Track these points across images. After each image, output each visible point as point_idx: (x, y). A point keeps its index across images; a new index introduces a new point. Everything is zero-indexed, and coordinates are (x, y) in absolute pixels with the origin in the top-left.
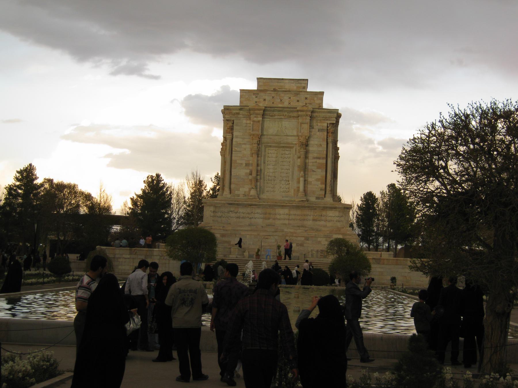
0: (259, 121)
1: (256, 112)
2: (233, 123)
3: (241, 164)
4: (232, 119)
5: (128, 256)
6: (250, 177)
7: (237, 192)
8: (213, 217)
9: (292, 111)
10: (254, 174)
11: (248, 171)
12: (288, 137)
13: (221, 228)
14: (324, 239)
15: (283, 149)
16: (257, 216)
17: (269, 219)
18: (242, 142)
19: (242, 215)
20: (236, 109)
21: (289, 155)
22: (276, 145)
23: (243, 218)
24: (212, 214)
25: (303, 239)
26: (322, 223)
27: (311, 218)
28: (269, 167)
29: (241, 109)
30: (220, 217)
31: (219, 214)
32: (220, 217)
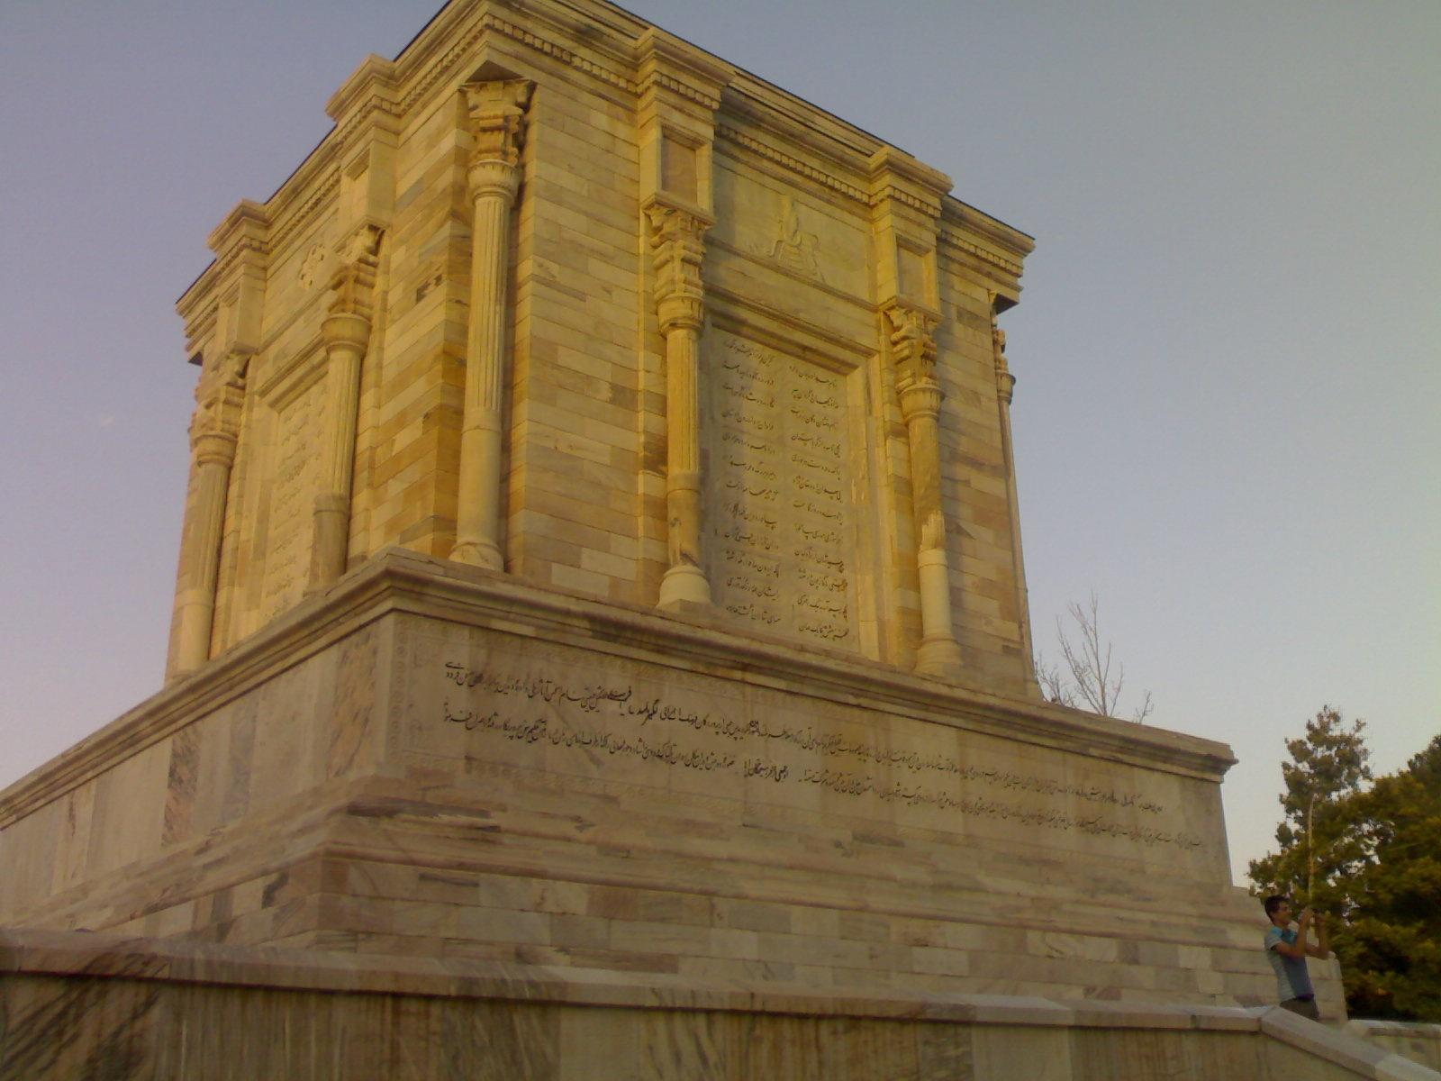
0: (694, 144)
1: (684, 78)
2: (526, 107)
3: (589, 379)
4: (529, 74)
6: (645, 483)
7: (560, 576)
8: (469, 723)
10: (682, 465)
12: (830, 301)
13: (569, 828)
15: (803, 366)
16: (782, 754)
17: (856, 790)
19: (687, 740)
20: (558, 24)
21: (829, 410)
22: (773, 326)
23: (693, 761)
24: (462, 701)
25: (1110, 950)
26: (1123, 847)
29: (585, 35)
30: (531, 734)
31: (516, 708)
32: (531, 734)
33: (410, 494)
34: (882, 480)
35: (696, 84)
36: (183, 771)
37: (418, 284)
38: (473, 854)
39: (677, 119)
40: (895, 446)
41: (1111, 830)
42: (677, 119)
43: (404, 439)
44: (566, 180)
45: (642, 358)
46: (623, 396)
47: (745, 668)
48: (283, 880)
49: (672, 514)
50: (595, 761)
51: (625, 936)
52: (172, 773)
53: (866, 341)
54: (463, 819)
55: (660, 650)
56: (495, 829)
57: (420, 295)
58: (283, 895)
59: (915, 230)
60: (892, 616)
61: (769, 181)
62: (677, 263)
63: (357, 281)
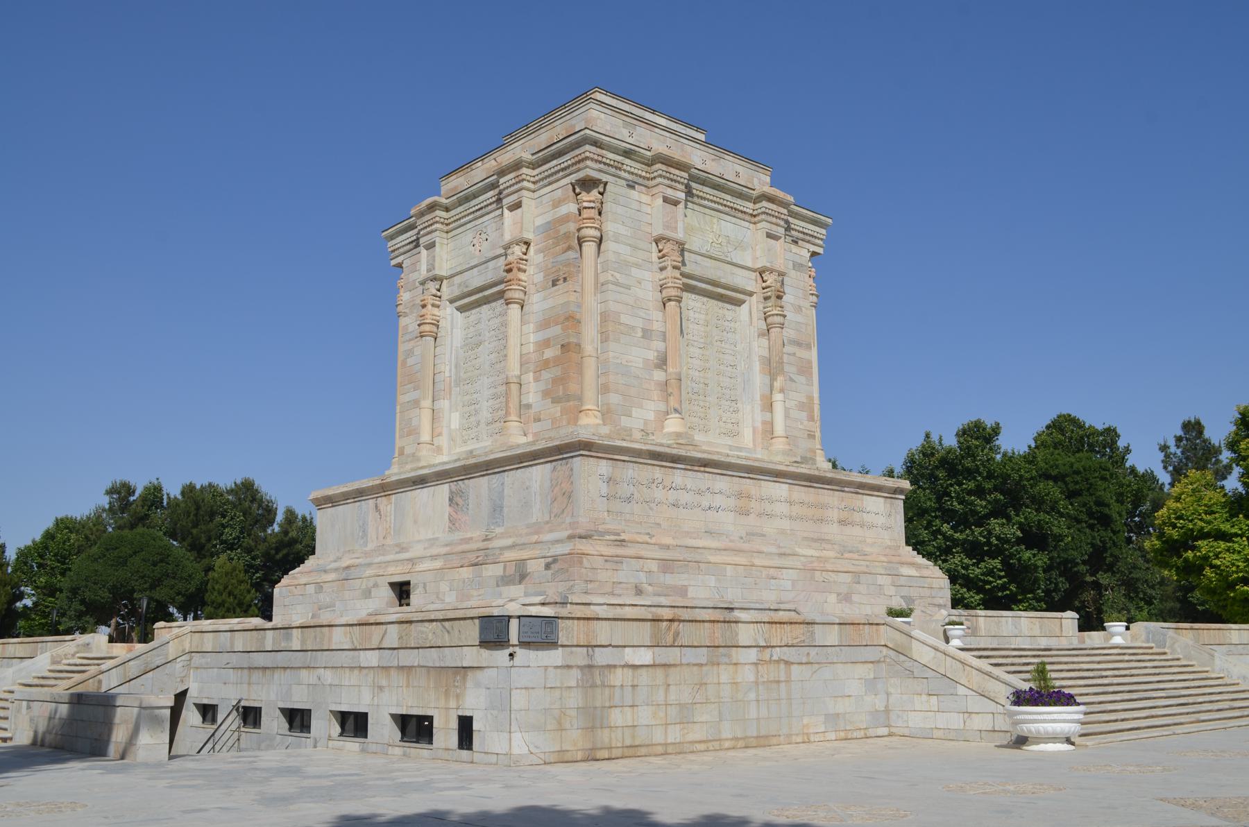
0: (675, 203)
3: (633, 328)
4: (604, 178)
5: (645, 656)
6: (659, 375)
7: (625, 422)
9: (741, 196)
11: (651, 355)
13: (647, 538)
14: (888, 580)
15: (720, 304)
16: (718, 501)
18: (631, 259)
19: (685, 497)
20: (615, 150)
21: (732, 325)
24: (604, 489)
26: (856, 531)
27: (834, 514)
28: (692, 349)
29: (627, 154)
30: (629, 500)
32: (629, 500)
33: (555, 381)
34: (757, 359)
35: (677, 172)
36: (460, 502)
37: (552, 277)
38: (620, 551)
39: (670, 192)
40: (764, 342)
41: (852, 524)
42: (670, 192)
43: (549, 353)
44: (622, 230)
45: (657, 315)
46: (647, 334)
47: (705, 466)
48: (555, 561)
49: (670, 390)
50: (651, 509)
51: (669, 579)
52: (451, 500)
53: (749, 288)
54: (613, 537)
55: (673, 462)
56: (623, 541)
57: (554, 283)
58: (555, 567)
59: (774, 228)
60: (759, 425)
61: (707, 211)
62: (669, 268)
63: (519, 269)
